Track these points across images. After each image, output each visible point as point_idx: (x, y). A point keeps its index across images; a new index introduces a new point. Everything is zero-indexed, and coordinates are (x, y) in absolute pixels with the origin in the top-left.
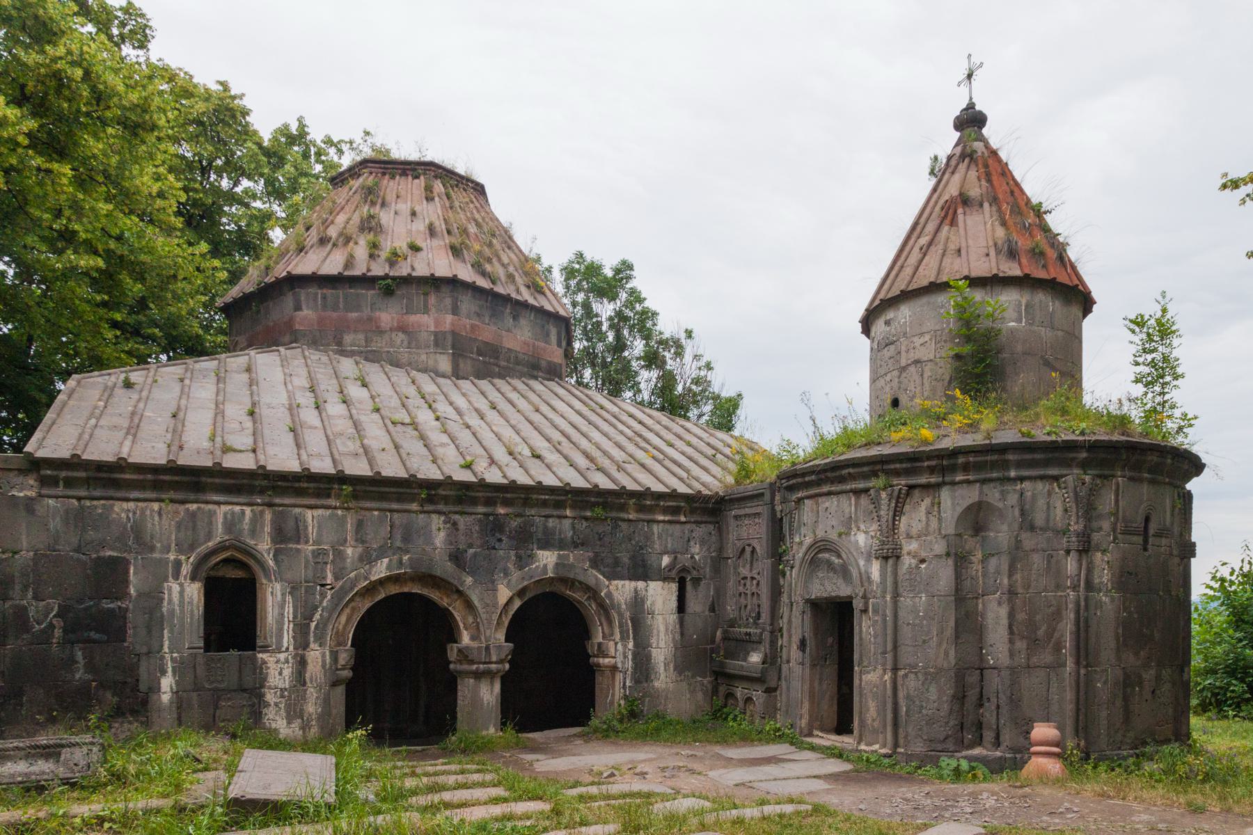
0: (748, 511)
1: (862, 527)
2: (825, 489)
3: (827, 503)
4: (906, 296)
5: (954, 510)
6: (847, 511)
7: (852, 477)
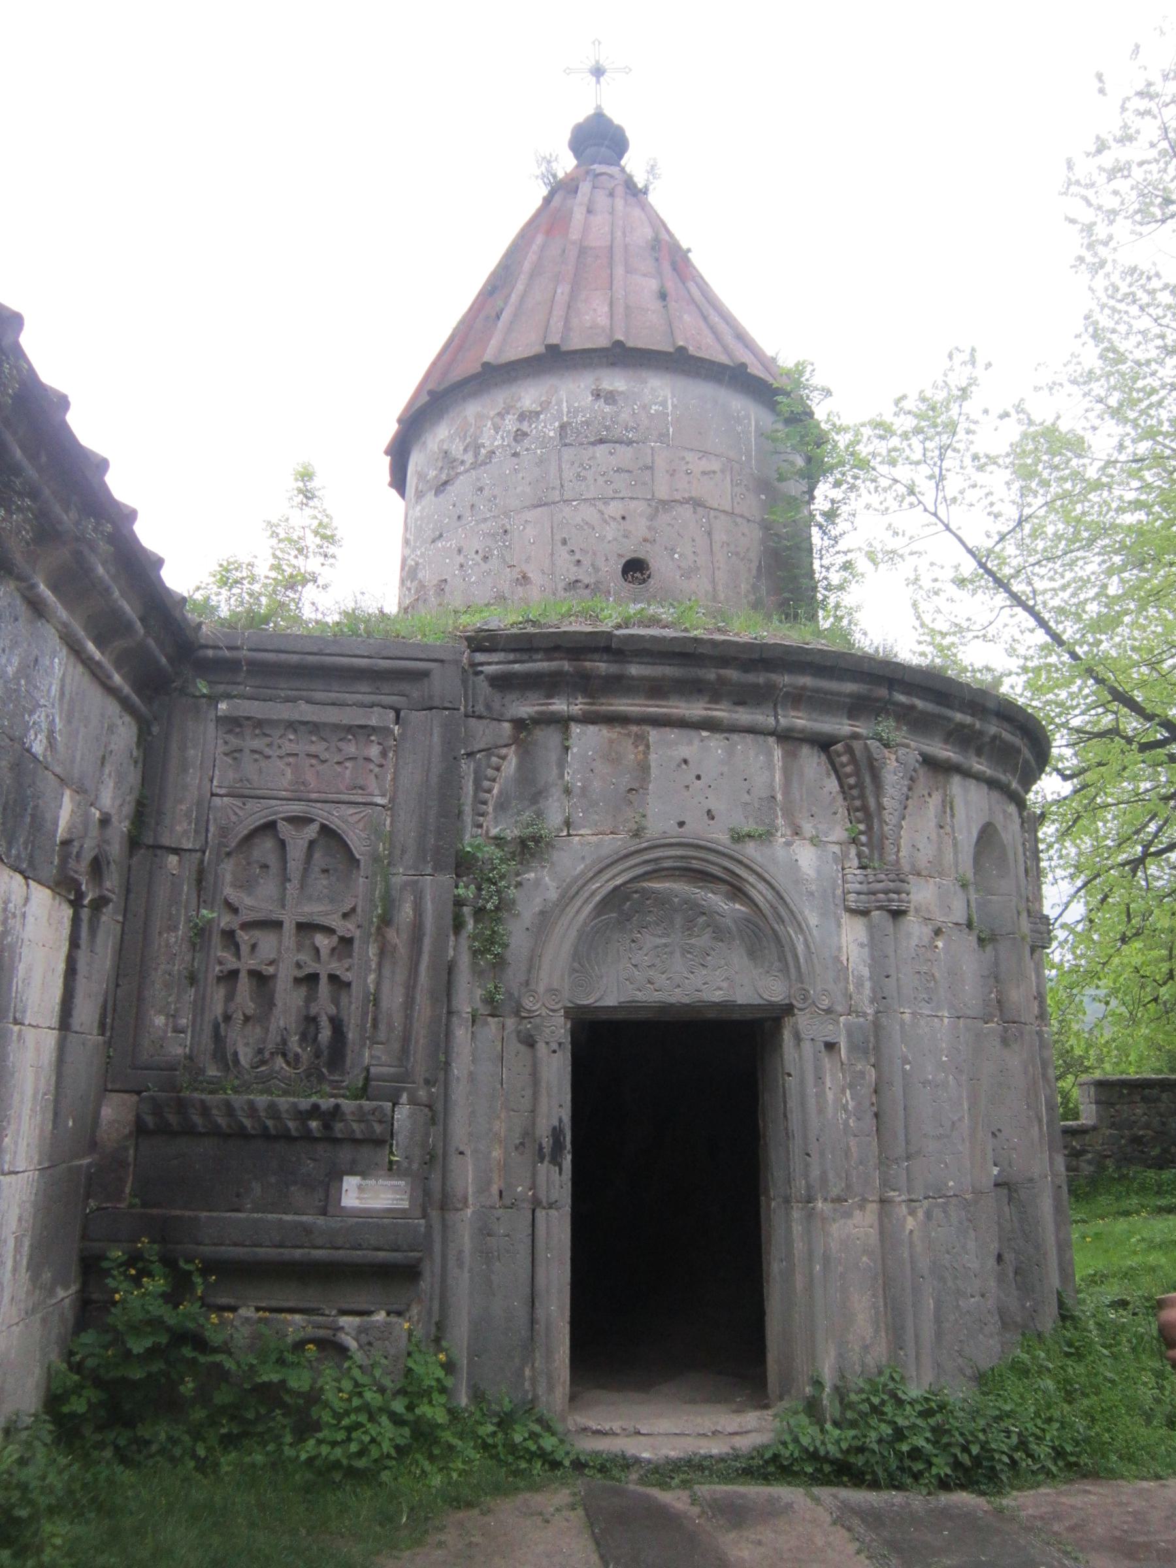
0: (305, 711)
1: (808, 828)
2: (696, 709)
3: (687, 746)
4: (497, 375)
5: (970, 832)
7: (797, 699)
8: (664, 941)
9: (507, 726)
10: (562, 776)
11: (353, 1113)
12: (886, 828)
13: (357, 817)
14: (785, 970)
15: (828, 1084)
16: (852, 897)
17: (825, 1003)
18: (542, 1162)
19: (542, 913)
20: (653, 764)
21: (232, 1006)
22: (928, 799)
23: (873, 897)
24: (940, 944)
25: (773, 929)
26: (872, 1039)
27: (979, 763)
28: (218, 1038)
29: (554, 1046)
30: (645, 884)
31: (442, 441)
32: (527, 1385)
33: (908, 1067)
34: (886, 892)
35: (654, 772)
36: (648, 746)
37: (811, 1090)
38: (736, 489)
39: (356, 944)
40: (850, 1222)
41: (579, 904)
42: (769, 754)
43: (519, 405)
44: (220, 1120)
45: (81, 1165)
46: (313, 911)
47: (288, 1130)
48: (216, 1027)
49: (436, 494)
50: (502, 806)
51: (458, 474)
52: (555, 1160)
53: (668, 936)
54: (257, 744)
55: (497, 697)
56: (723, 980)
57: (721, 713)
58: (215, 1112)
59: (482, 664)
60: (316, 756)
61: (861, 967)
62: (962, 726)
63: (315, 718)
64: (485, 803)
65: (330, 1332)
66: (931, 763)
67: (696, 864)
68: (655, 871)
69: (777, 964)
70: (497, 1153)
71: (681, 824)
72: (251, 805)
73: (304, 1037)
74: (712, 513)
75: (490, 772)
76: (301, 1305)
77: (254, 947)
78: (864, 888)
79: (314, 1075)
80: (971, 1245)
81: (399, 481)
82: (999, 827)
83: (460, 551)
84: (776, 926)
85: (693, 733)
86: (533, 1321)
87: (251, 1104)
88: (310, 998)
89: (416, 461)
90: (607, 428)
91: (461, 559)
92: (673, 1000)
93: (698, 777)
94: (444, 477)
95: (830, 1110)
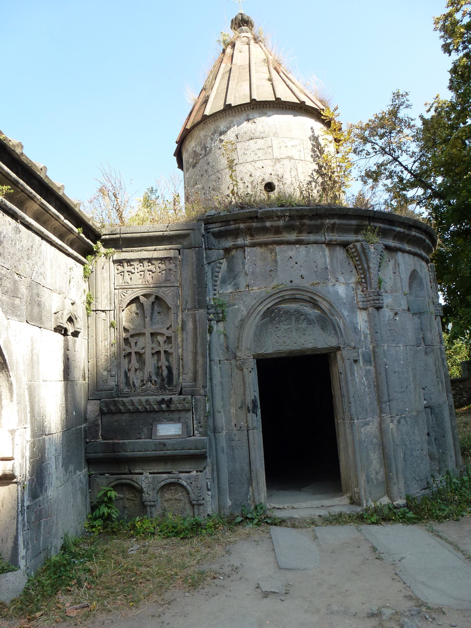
1: (341, 279)
2: (293, 237)
3: (291, 251)
6: (320, 262)
7: (332, 228)
8: (288, 327)
9: (222, 252)
10: (244, 268)
11: (177, 401)
12: (372, 276)
13: (169, 291)
14: (336, 333)
15: (356, 376)
16: (361, 303)
17: (353, 344)
18: (249, 413)
19: (241, 320)
20: (278, 260)
21: (130, 366)
22: (388, 262)
23: (368, 303)
24: (397, 319)
25: (331, 319)
26: (372, 357)
27: (409, 247)
28: (127, 377)
29: (251, 370)
30: (279, 306)
31: (193, 147)
32: (251, 494)
33: (387, 367)
34: (374, 300)
35: (279, 263)
36: (276, 253)
37: (350, 378)
38: (305, 151)
39: (173, 339)
40: (368, 427)
41: (255, 315)
42: (324, 251)
43: (219, 129)
44: (129, 407)
45: (81, 428)
46: (156, 328)
47: (154, 408)
48: (126, 373)
49: (193, 168)
50: (224, 282)
51: (200, 159)
52: (254, 412)
53: (290, 324)
54: (130, 268)
55: (217, 241)
56: (312, 339)
57: (304, 237)
58: (127, 404)
59: (209, 229)
60: (151, 271)
61: (366, 330)
62: (399, 232)
63: (150, 257)
64: (217, 281)
65: (177, 480)
66: (388, 248)
67: (298, 296)
68: (282, 301)
69: (333, 331)
70: (233, 411)
71: (291, 282)
72: (130, 291)
73: (157, 374)
74: (297, 161)
75: (217, 269)
76: (165, 471)
77: (136, 343)
78: (365, 299)
79: (162, 387)
80: (417, 432)
81: (181, 165)
82: (419, 271)
83: (203, 188)
84: (331, 317)
85: (293, 246)
86: (251, 471)
87: (140, 400)
88: (159, 360)
89: (185, 156)
90: (253, 134)
91: (204, 191)
92: (293, 349)
93: (296, 263)
94: (195, 161)
95: (358, 385)
